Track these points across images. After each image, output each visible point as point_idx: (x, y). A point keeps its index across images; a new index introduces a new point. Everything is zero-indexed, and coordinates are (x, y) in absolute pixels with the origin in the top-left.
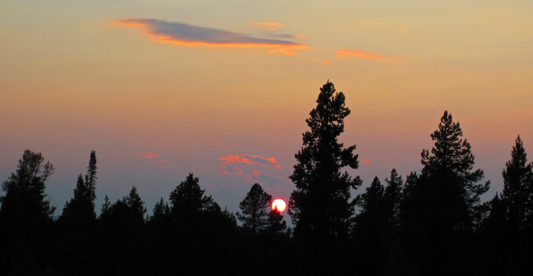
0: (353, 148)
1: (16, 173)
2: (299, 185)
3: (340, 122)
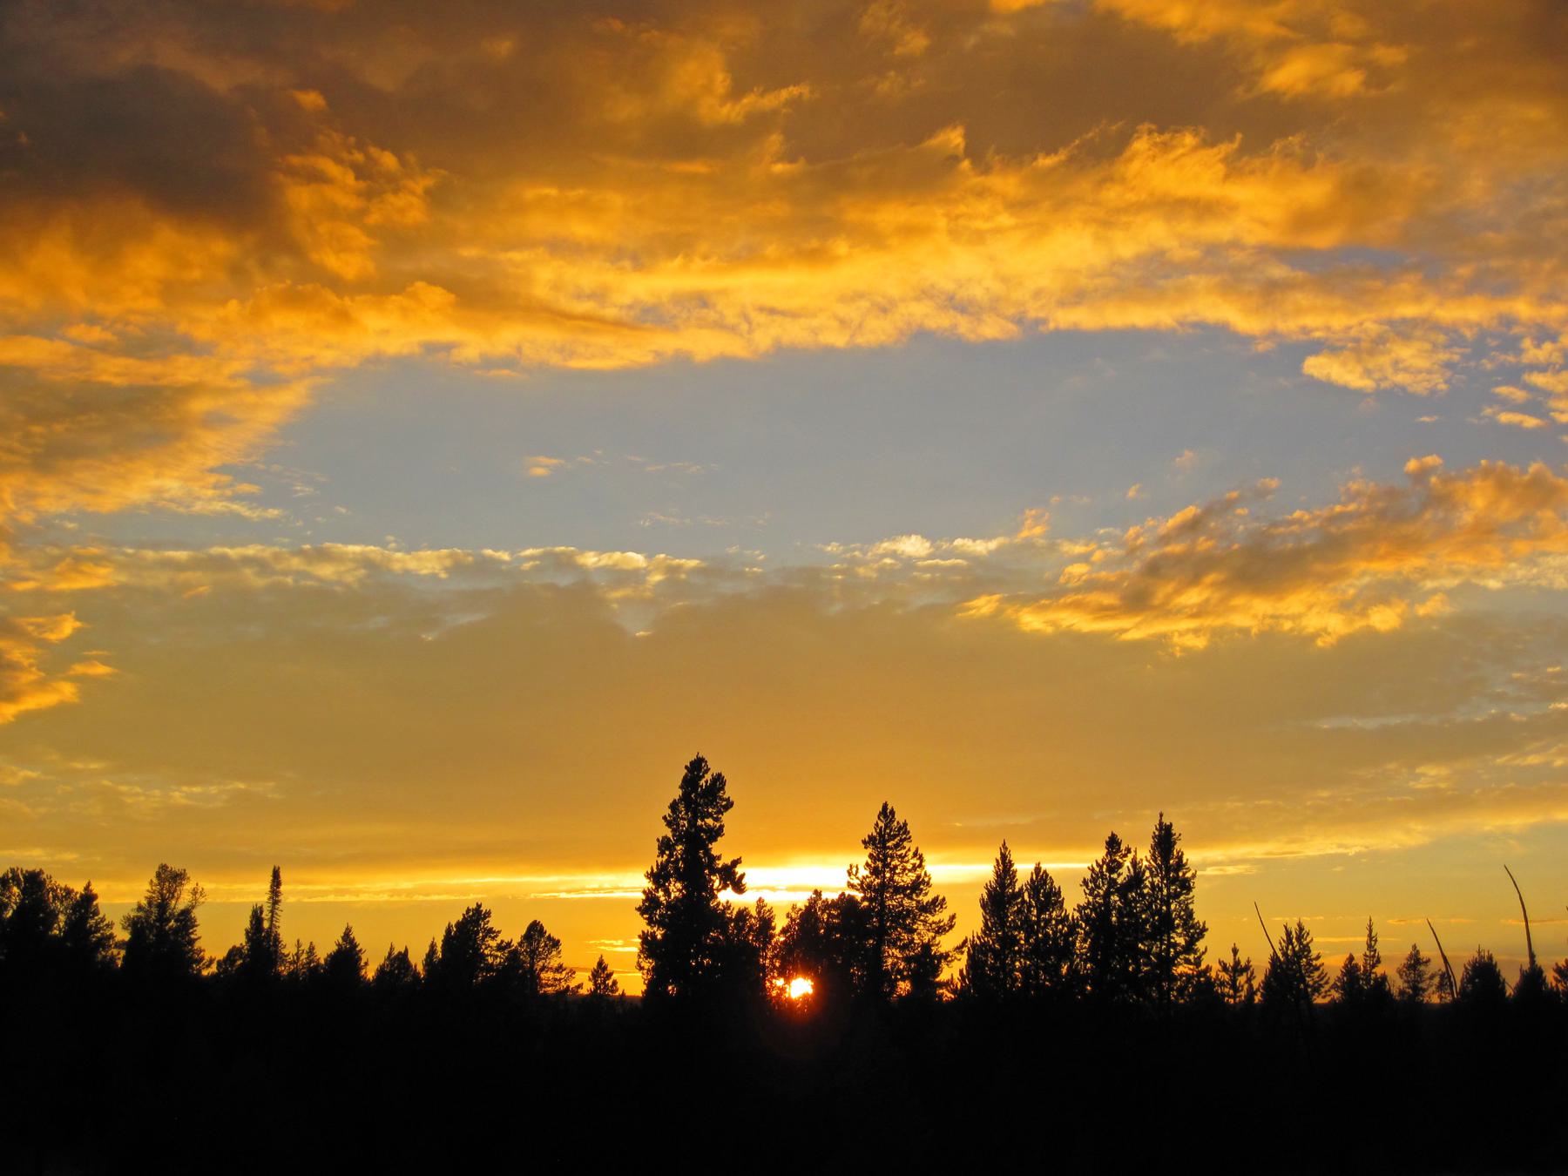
0: (736, 863)
2: (650, 922)
3: (716, 820)
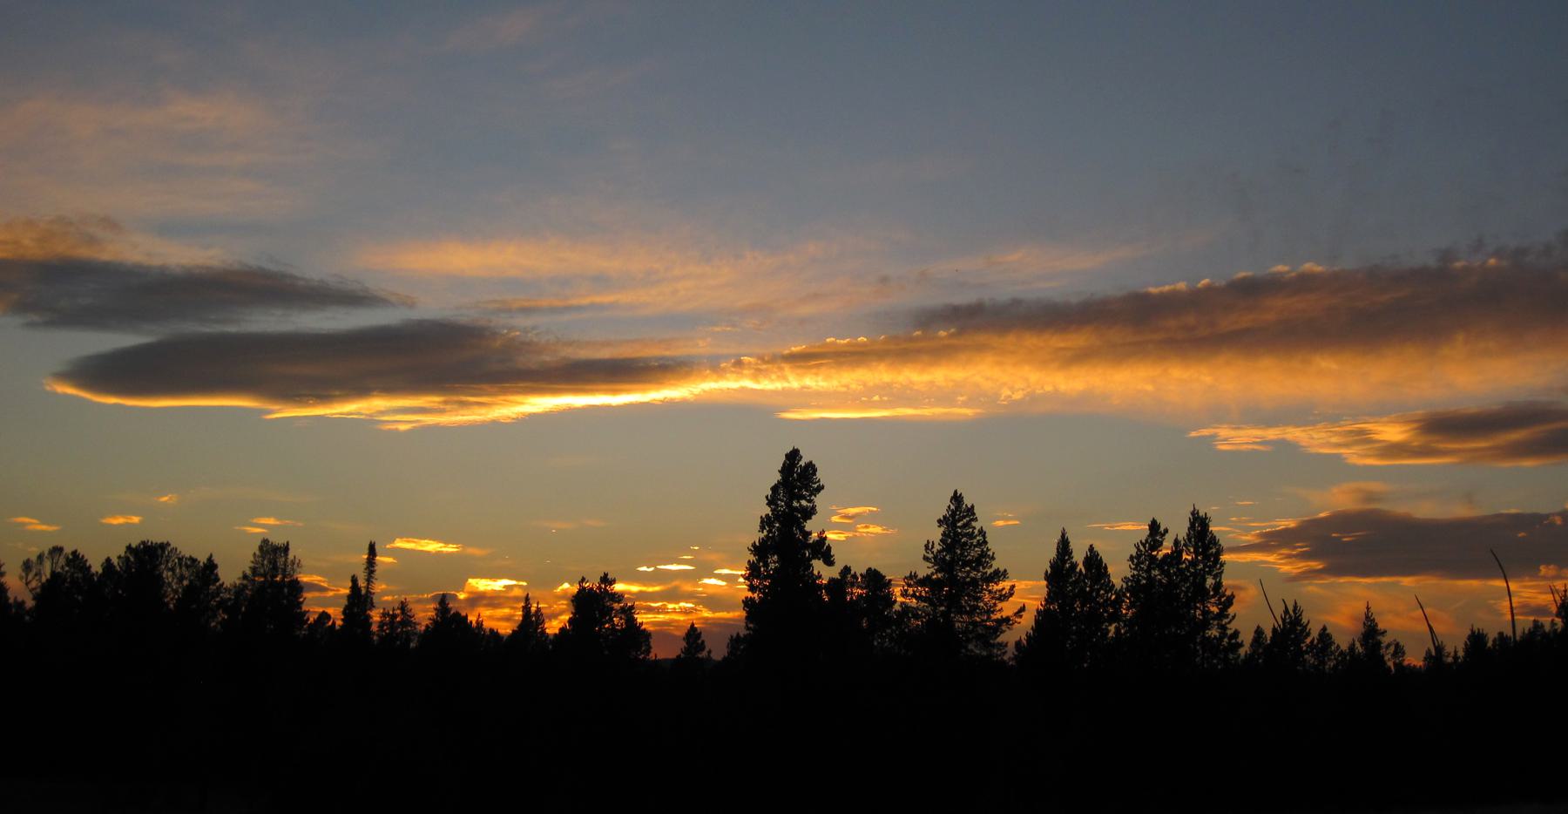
1: (249, 572)
2: (752, 588)
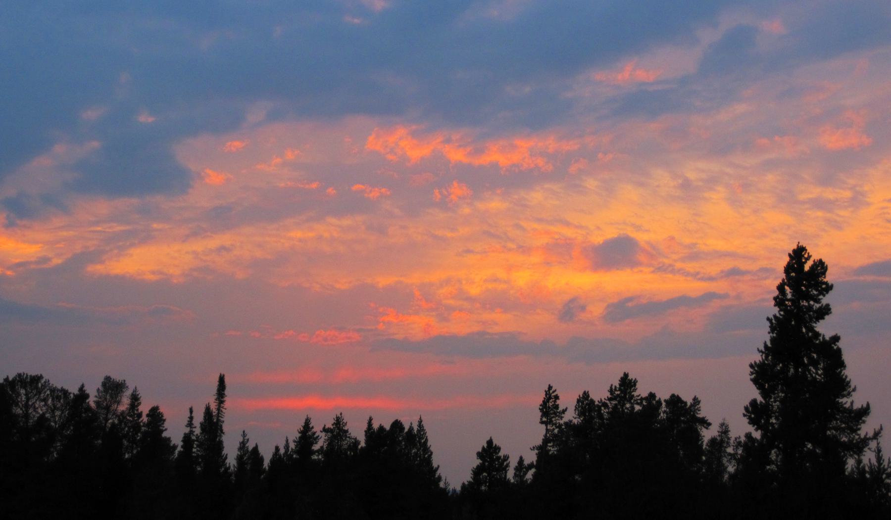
0: (836, 339)
